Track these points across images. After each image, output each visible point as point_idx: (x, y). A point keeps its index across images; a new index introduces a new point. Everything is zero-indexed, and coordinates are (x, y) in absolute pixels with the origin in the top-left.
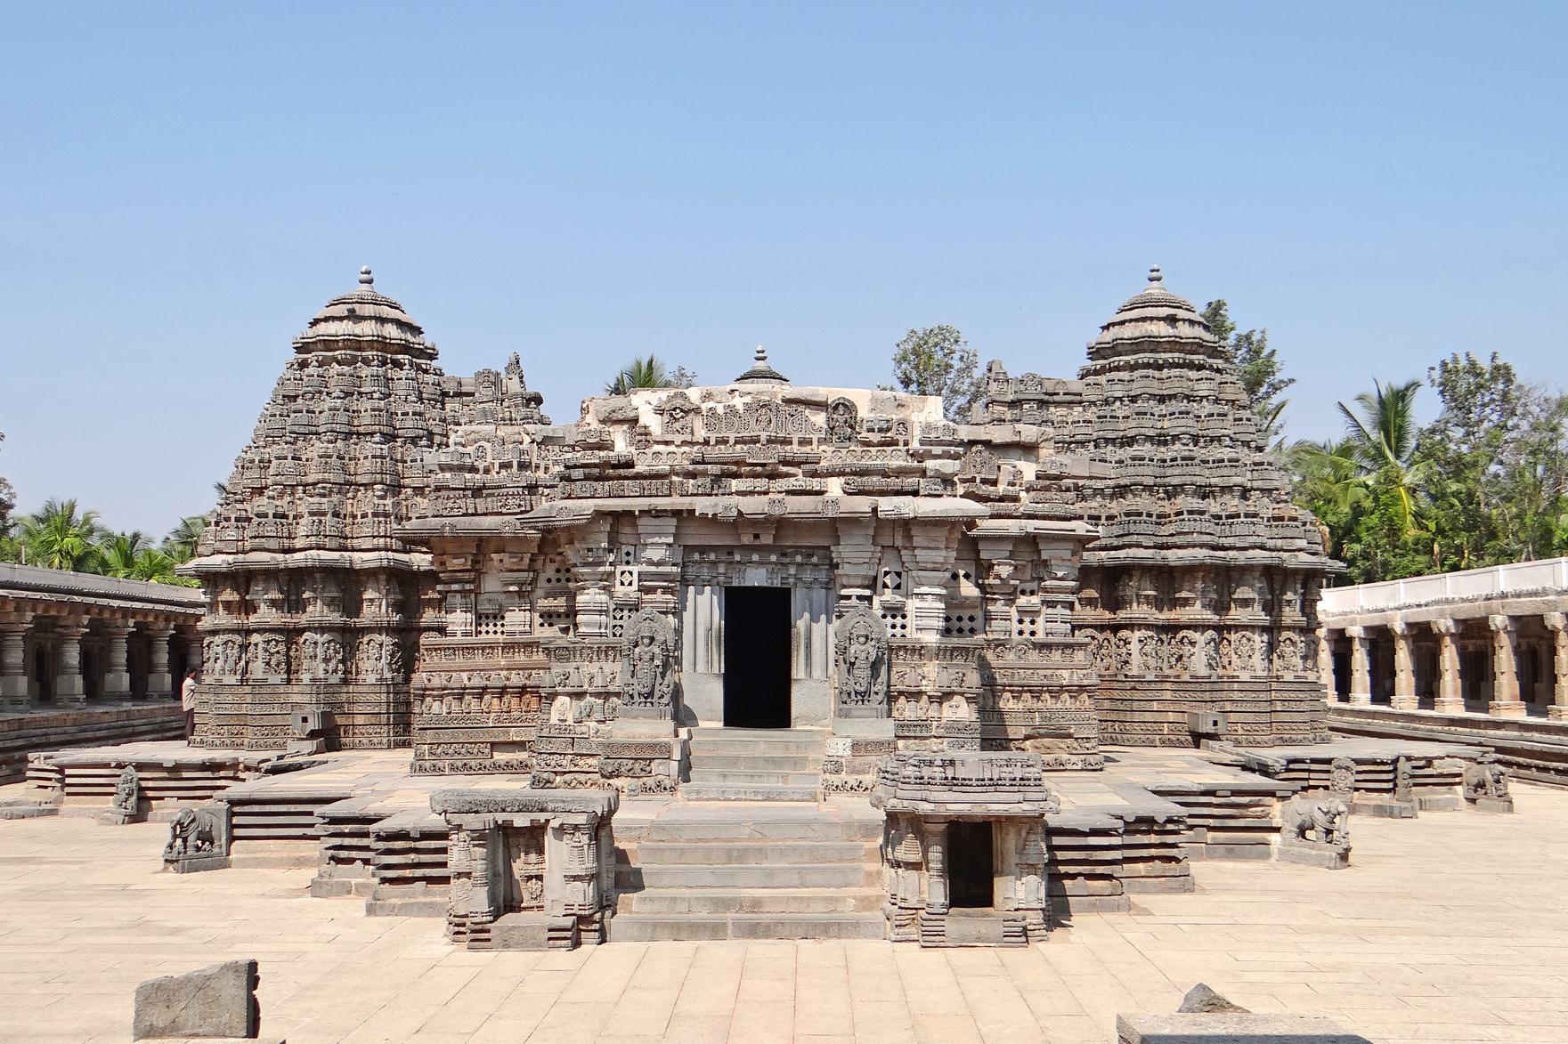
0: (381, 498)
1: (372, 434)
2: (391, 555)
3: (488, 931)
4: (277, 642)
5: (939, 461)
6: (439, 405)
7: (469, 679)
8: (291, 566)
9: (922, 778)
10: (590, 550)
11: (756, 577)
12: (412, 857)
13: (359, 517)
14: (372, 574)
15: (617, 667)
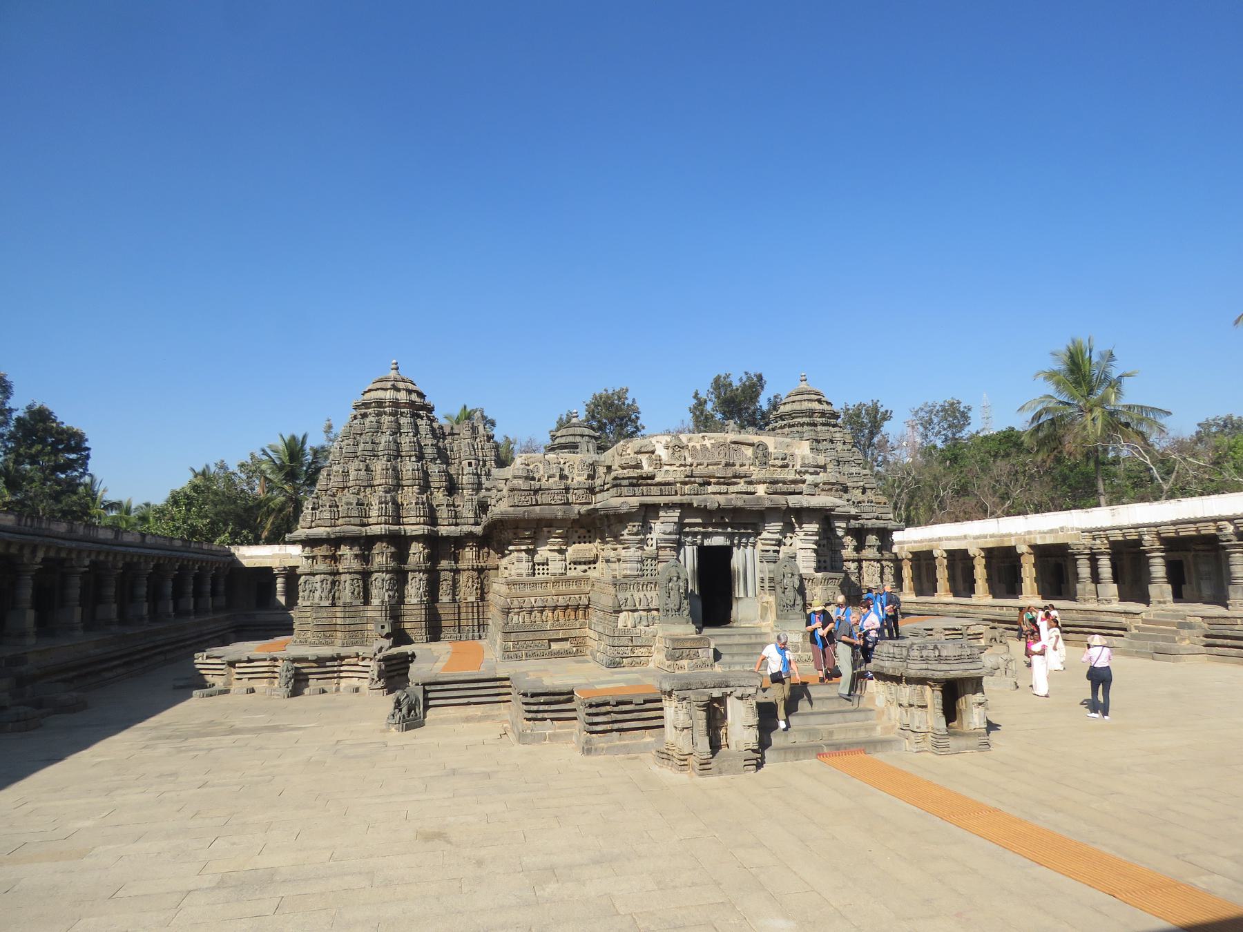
0: (419, 493)
1: (410, 456)
2: (429, 528)
3: (710, 763)
4: (358, 579)
5: (814, 476)
6: (441, 440)
7: (535, 602)
8: (369, 534)
9: (922, 657)
10: (634, 526)
11: (718, 541)
12: (614, 717)
13: (405, 505)
14: (416, 538)
15: (654, 594)
